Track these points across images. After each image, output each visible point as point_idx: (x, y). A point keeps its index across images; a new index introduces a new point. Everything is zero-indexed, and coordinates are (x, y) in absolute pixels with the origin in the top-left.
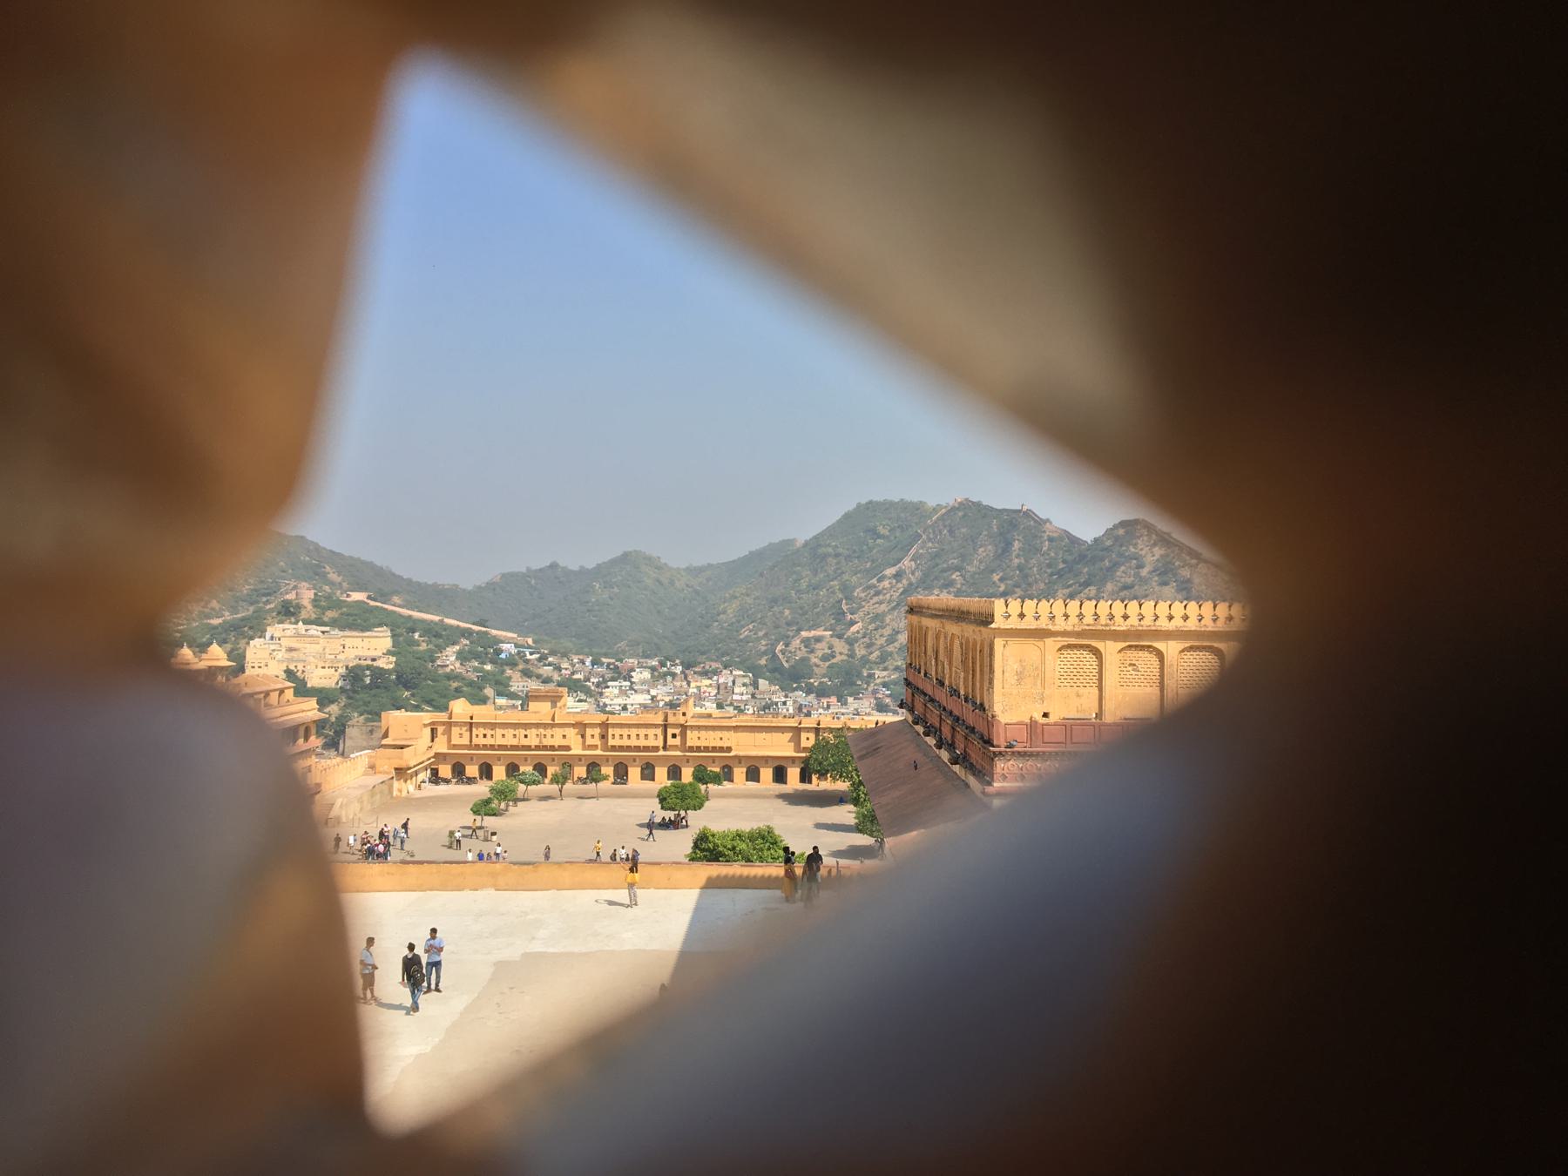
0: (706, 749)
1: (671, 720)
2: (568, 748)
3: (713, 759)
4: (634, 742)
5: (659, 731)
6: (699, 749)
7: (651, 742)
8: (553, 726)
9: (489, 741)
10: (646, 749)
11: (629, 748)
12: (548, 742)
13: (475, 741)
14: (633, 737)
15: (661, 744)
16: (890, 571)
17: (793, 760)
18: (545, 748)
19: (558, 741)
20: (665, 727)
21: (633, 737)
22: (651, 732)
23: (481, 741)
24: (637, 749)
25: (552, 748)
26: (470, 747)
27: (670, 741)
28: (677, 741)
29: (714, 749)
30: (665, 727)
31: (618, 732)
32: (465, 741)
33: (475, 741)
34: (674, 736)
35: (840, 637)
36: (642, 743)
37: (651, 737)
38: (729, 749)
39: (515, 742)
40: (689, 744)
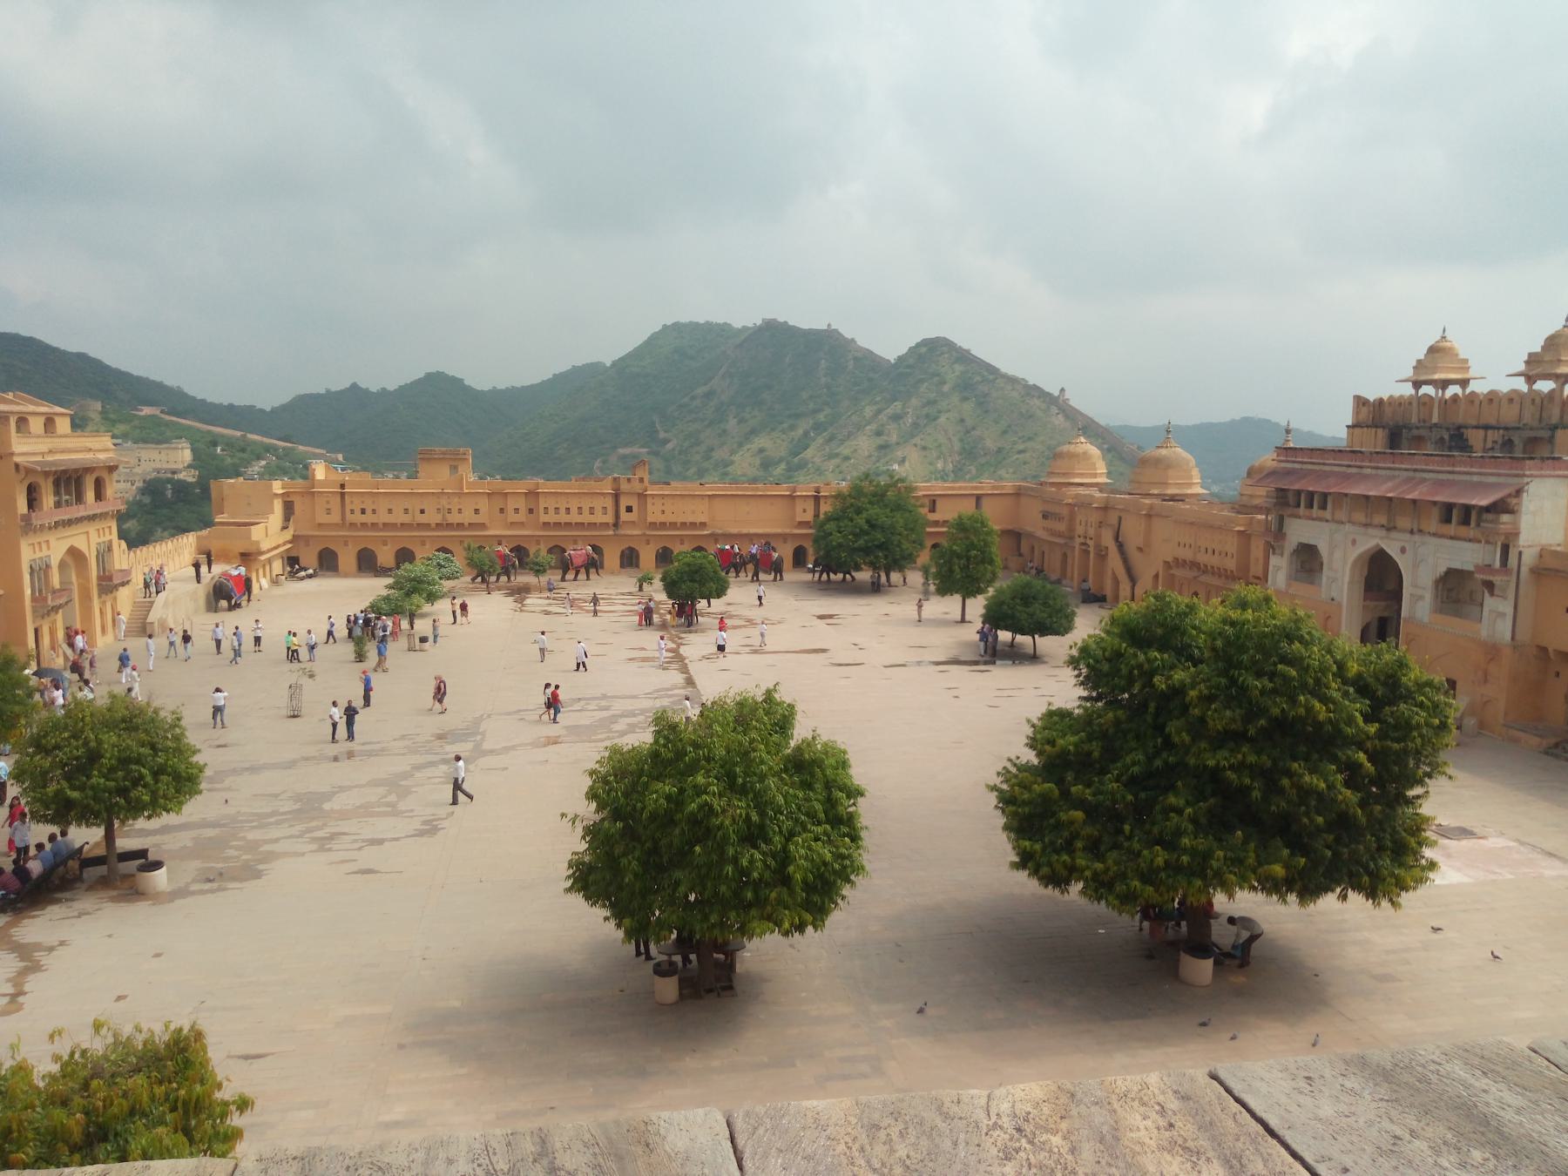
0: (673, 525)
1: (624, 486)
2: (482, 526)
3: (682, 539)
4: (574, 518)
5: (609, 503)
6: (663, 525)
7: (599, 518)
8: (460, 495)
9: (368, 518)
10: (592, 526)
11: (568, 525)
12: (455, 518)
13: (350, 518)
14: (574, 510)
15: (609, 519)
16: (700, 391)
17: (784, 537)
18: (449, 526)
19: (467, 517)
20: (616, 497)
21: (574, 510)
22: (598, 504)
23: (358, 518)
24: (580, 525)
25: (460, 526)
26: (343, 524)
27: (624, 516)
28: (632, 517)
29: (684, 524)
30: (616, 497)
31: (551, 503)
32: (335, 518)
33: (349, 516)
34: (629, 509)
35: (656, 454)
36: (586, 518)
37: (599, 511)
38: (703, 525)
39: (406, 519)
40: (650, 519)
